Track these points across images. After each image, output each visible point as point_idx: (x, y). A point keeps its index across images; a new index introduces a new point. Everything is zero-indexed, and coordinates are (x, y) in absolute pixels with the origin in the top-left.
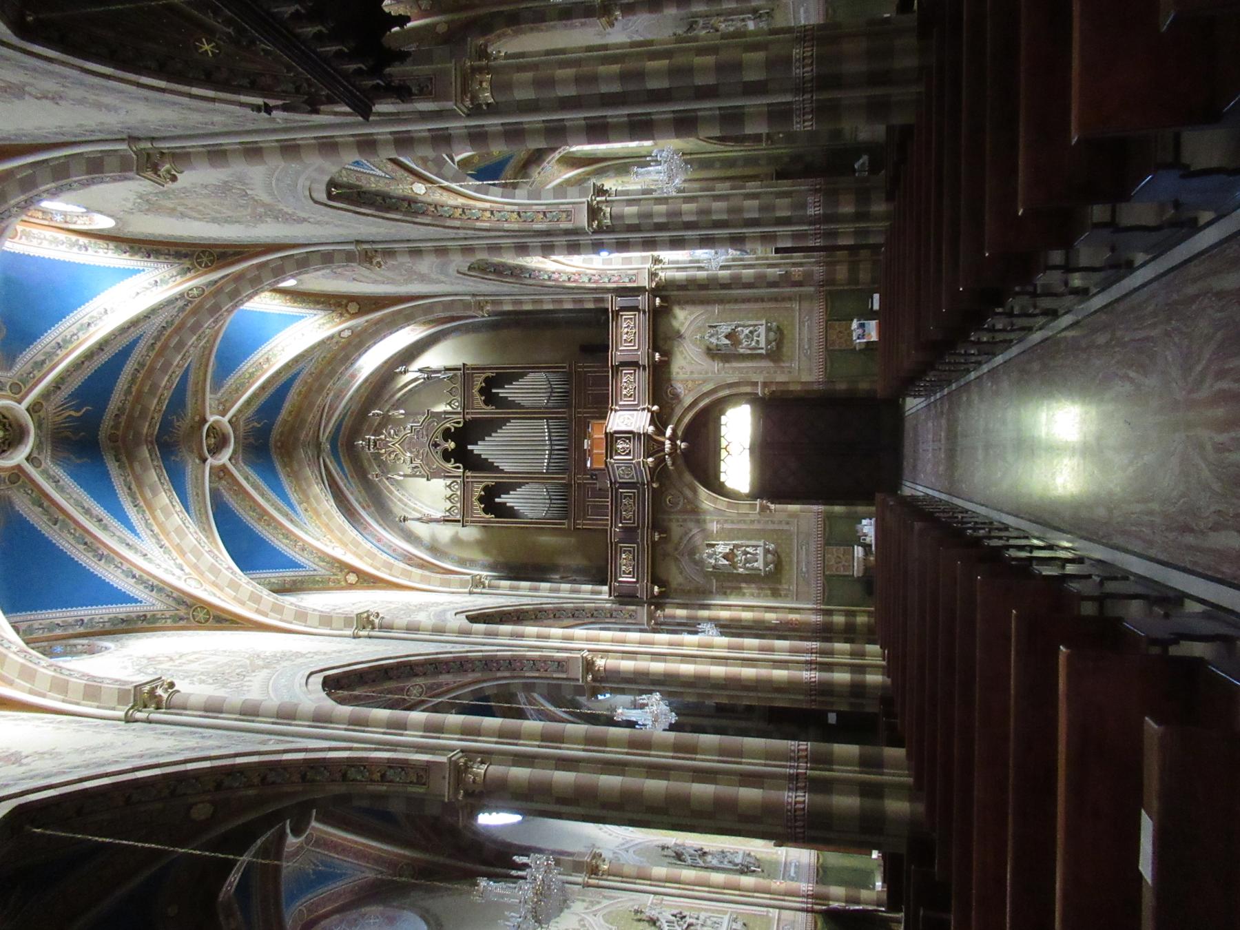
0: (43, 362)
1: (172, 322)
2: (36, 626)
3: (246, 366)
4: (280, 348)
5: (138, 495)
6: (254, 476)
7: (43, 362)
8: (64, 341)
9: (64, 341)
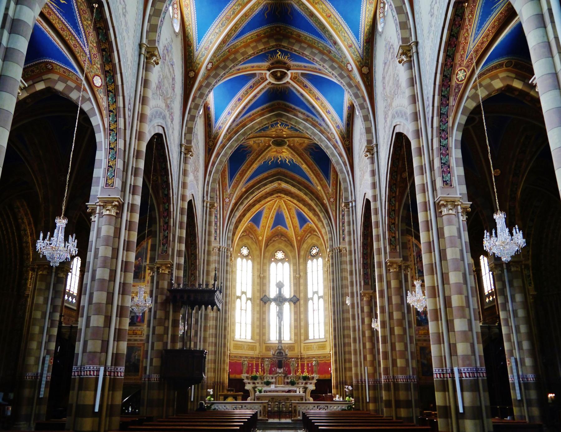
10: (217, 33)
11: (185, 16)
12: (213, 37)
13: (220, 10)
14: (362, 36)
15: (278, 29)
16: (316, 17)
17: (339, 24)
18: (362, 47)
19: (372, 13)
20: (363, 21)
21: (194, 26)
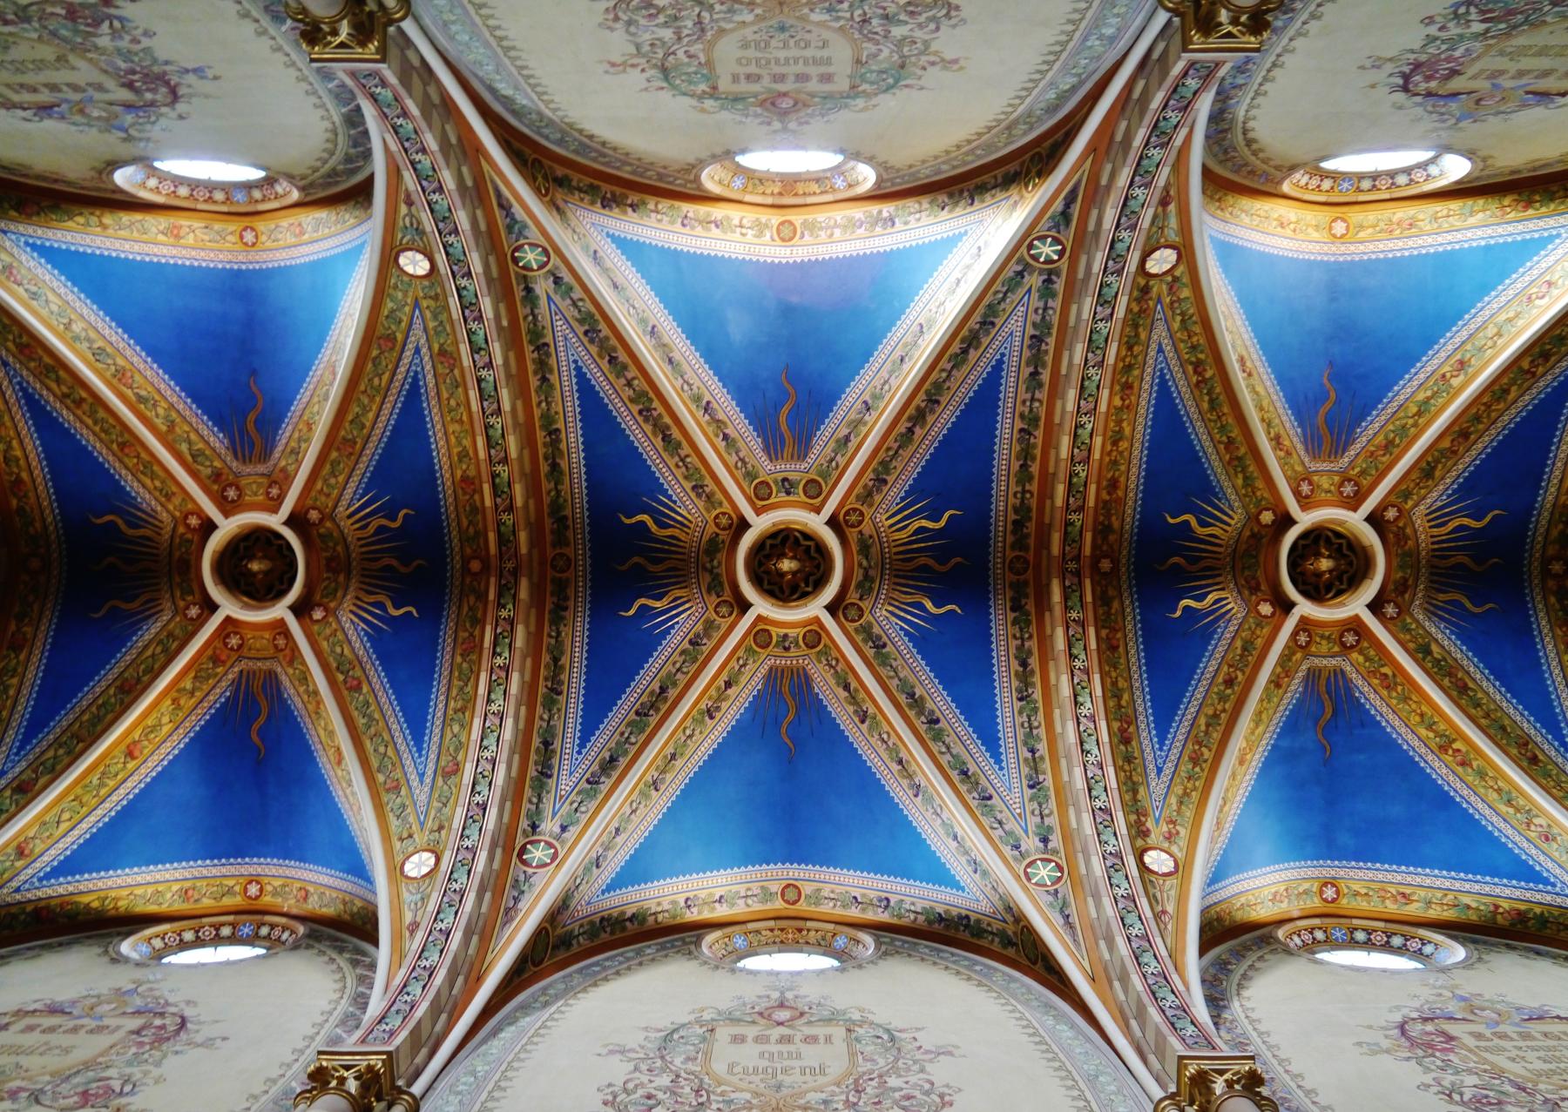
0: (847, 439)
1: (1044, 326)
2: (825, 893)
3: (1409, 389)
4: (1491, 331)
5: (1037, 679)
6: (1445, 640)
7: (847, 439)
9: (874, 397)
10: (68, 326)
11: (138, 216)
12: (55, 308)
13: (154, 352)
14: (61, 890)
15: (35, 564)
16: (125, 708)
17: (103, 792)
18: (18, 897)
19: (152, 908)
20: (119, 881)
21: (98, 241)
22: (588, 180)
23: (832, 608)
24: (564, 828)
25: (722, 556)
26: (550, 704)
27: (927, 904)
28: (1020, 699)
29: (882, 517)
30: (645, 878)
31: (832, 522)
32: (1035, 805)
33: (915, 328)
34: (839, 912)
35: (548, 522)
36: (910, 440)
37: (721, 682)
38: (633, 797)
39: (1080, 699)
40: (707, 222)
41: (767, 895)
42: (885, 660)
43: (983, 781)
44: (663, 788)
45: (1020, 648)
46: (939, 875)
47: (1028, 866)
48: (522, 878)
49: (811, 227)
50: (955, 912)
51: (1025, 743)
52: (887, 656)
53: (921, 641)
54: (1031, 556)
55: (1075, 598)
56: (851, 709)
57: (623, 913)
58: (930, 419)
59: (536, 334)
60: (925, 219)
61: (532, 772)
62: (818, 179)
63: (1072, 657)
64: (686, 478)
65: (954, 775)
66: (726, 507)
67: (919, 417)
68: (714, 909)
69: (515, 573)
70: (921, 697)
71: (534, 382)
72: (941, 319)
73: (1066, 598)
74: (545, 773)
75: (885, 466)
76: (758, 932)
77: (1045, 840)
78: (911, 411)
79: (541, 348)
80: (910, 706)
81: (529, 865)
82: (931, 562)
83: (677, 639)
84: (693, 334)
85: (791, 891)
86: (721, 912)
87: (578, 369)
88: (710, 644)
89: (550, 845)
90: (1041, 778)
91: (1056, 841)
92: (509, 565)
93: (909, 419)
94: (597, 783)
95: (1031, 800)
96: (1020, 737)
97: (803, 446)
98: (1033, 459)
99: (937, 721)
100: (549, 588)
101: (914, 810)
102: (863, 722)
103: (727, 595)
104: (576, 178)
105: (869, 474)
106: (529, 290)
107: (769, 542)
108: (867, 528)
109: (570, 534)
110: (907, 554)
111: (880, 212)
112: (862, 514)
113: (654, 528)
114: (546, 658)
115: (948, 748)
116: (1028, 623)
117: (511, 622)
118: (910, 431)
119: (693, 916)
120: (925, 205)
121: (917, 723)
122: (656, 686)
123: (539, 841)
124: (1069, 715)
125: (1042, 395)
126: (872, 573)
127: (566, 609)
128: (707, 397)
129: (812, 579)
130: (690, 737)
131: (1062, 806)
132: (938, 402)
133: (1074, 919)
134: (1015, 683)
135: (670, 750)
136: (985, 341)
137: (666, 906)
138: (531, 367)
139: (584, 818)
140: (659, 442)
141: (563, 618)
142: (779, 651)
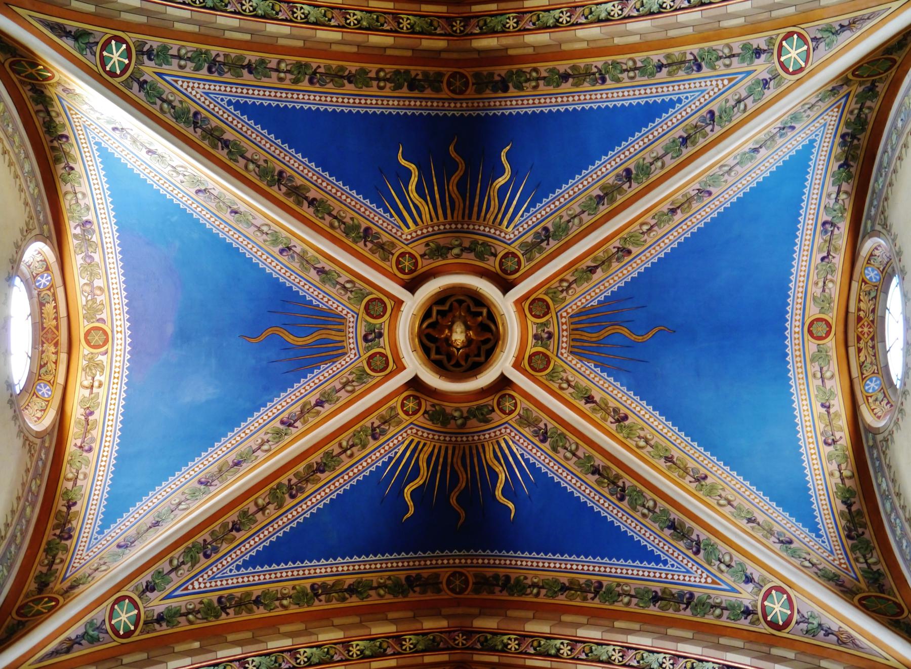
0: (321, 271)
1: (197, 59)
2: (818, 291)
5: (582, 63)
7: (321, 271)
8: (275, 242)
22: (41, 554)
23: (505, 287)
24: (749, 580)
25: (449, 407)
26: (612, 595)
27: (829, 180)
28: (604, 81)
29: (406, 233)
30: (803, 489)
31: (412, 286)
32: (720, 63)
33: (201, 198)
34: (838, 276)
35: (413, 597)
36: (322, 202)
37: (587, 408)
38: (713, 503)
39: (603, 15)
40: (87, 424)
41: (821, 355)
42: (562, 229)
43: (694, 120)
44: (703, 471)
45: (548, 81)
46: (797, 167)
47: (786, 70)
48: (804, 626)
49: (92, 311)
50: (837, 150)
51: (652, 75)
52: (558, 227)
53: (540, 189)
54: (447, 71)
55: (492, 22)
56: (615, 265)
57: (842, 514)
58: (299, 181)
59: (209, 611)
60: (83, 187)
61: (686, 615)
62: (39, 303)
63: (557, 25)
64: (364, 447)
65: (687, 152)
66: (396, 402)
67: (297, 193)
68: (837, 414)
69: (469, 633)
70: (602, 188)
71: (260, 613)
72: (191, 170)
73: (493, 32)
74: (687, 600)
75: (349, 230)
76: (861, 365)
77: (758, 52)
78: (290, 202)
79: (223, 605)
80: (612, 200)
81: (790, 618)
82: (455, 179)
83: (541, 457)
84: (209, 440)
85: (815, 329)
86: (840, 405)
87: (246, 565)
88: (545, 419)
89: (767, 595)
90: (690, 57)
91: (759, 40)
92: (460, 639)
93: (299, 204)
94: (698, 543)
95: (714, 68)
96: (645, 80)
97: (330, 319)
98: (342, 69)
99: (628, 171)
100: (485, 596)
101: (727, 195)
102: (629, 252)
103: (492, 401)
104: (38, 568)
105: (359, 247)
106: (160, 619)
107: (434, 356)
108: (418, 249)
109: (425, 573)
110: (446, 205)
111: (75, 236)
112: (402, 255)
113: (419, 482)
114: (561, 599)
115: (657, 159)
116: (520, 72)
117: (523, 637)
118: (312, 202)
119: (844, 437)
120: (68, 187)
121: (630, 193)
122: (592, 479)
123: (763, 607)
124: (620, 28)
125: (273, 60)
126: (467, 244)
127: (508, 578)
128: (276, 424)
129: (473, 309)
130: (647, 441)
131: (720, 34)
132: (281, 173)
133: (845, 19)
134: (586, 86)
135: (661, 463)
136: (215, 122)
137: (834, 467)
138: (245, 616)
139: (737, 557)
140: (325, 477)
141: (518, 581)
142: (552, 344)
